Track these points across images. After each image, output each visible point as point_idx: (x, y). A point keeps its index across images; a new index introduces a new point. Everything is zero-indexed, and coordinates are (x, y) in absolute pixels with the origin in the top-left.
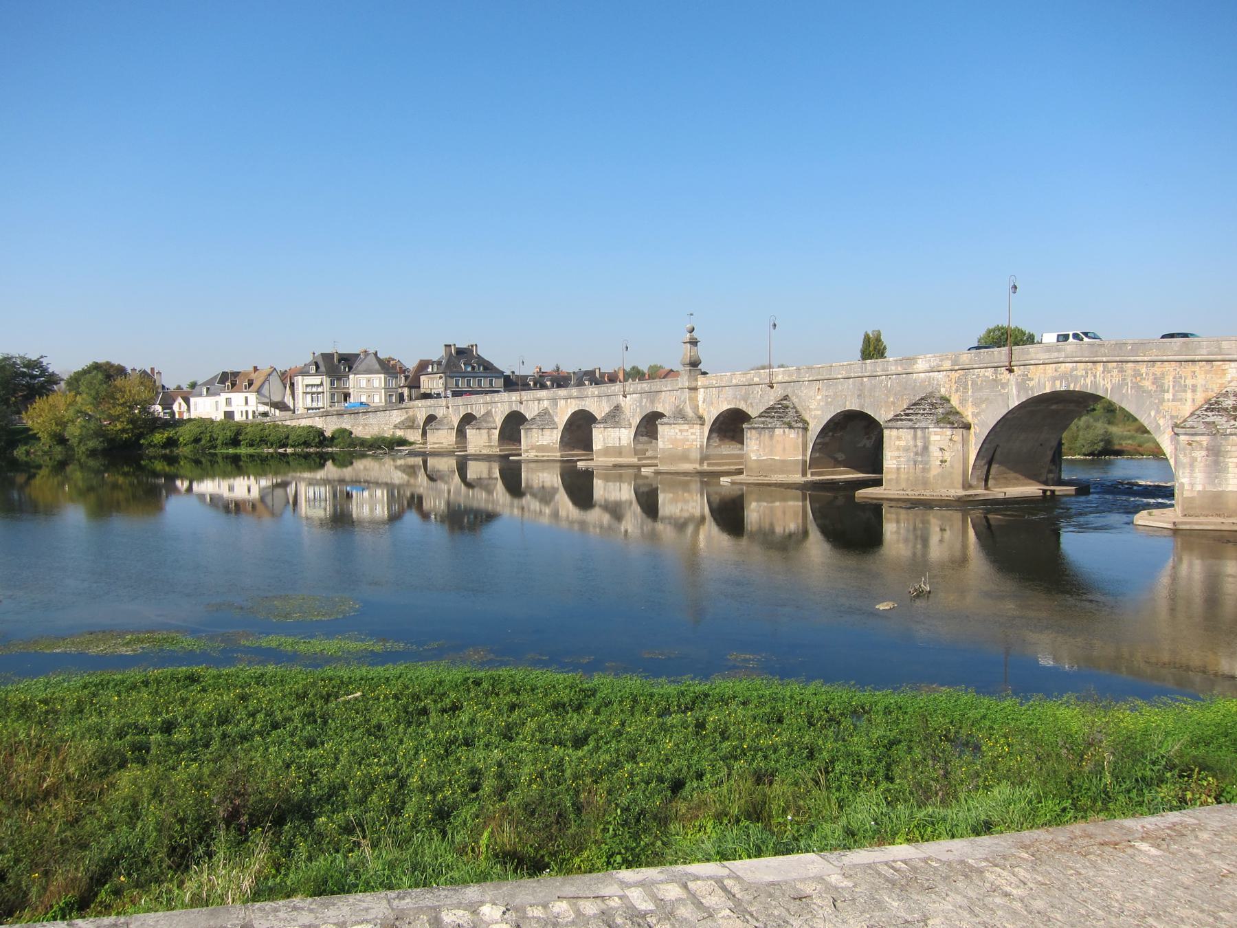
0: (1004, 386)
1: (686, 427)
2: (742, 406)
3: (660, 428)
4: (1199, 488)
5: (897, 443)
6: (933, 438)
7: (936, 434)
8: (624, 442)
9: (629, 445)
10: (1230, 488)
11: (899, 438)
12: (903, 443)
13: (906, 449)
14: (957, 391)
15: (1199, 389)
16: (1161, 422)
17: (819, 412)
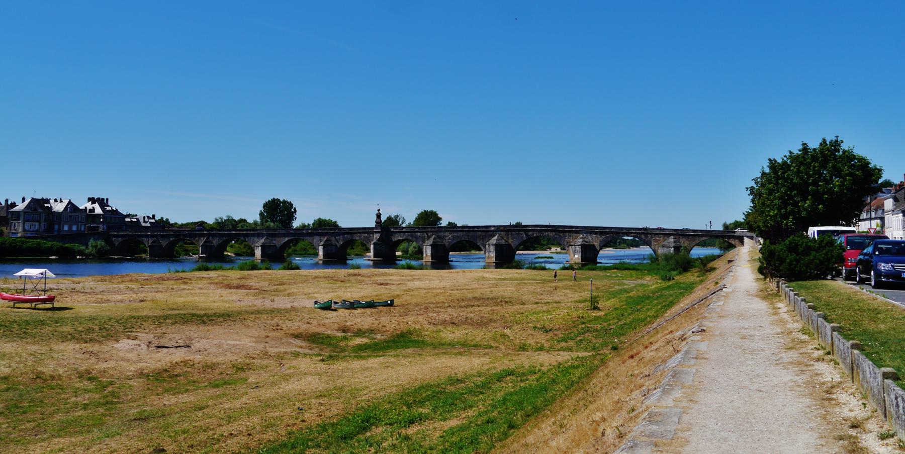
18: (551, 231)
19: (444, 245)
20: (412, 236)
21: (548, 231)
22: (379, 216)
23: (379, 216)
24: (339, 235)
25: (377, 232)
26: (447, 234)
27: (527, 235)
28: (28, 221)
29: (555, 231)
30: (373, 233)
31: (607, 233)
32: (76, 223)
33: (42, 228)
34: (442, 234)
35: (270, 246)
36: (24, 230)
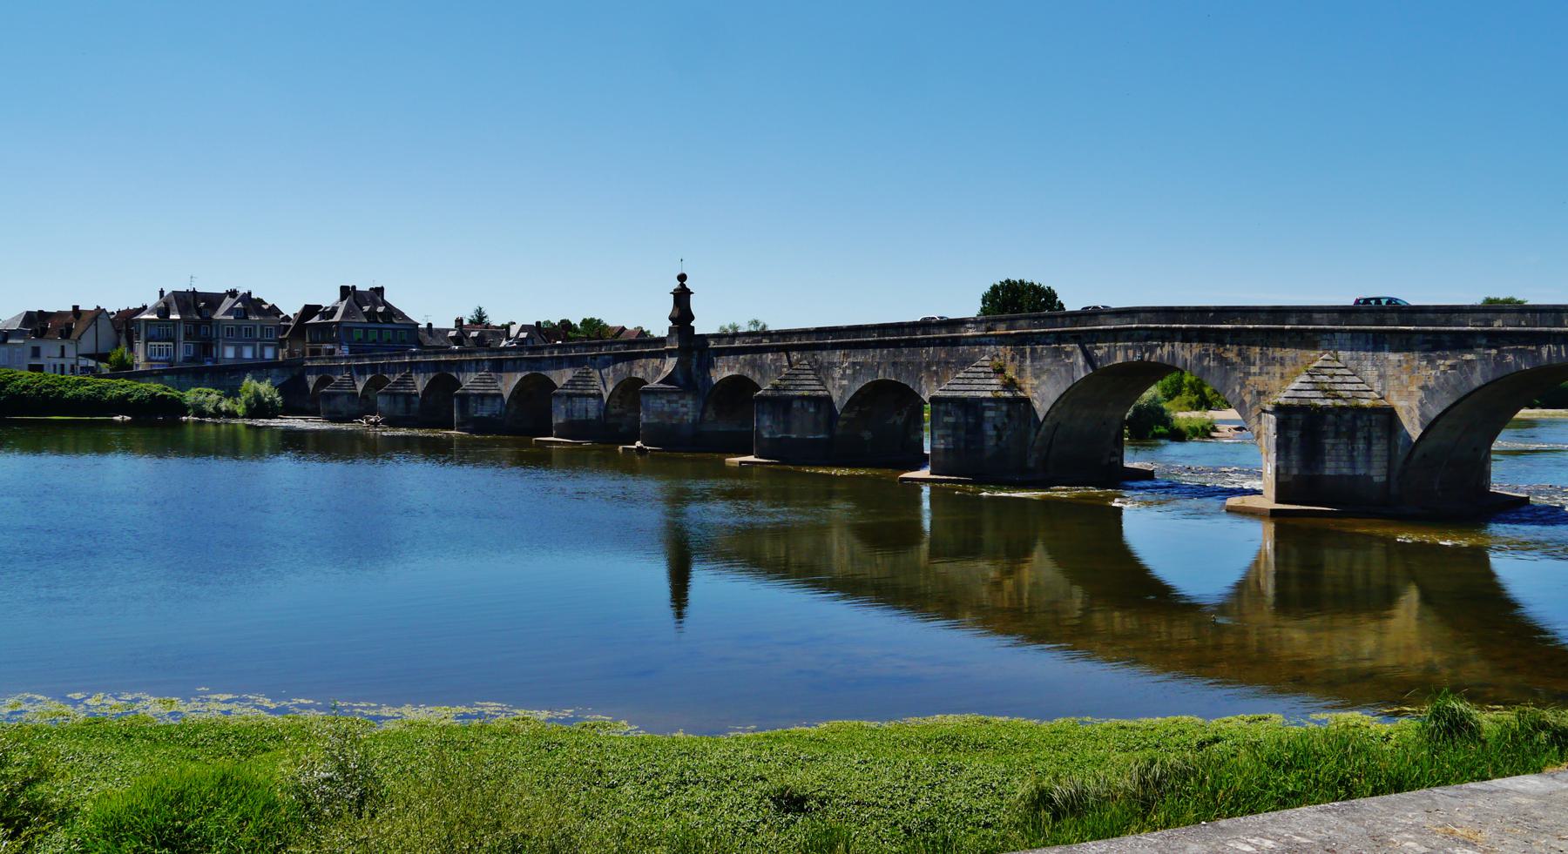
0: (1068, 355)
1: (675, 397)
2: (748, 373)
3: (643, 398)
4: (1295, 472)
5: (947, 419)
6: (989, 414)
7: (990, 409)
8: (592, 415)
9: (599, 417)
10: (1327, 472)
11: (947, 414)
12: (950, 420)
13: (955, 427)
14: (1013, 359)
15: (1288, 362)
16: (1248, 398)
17: (845, 382)
18: (1187, 337)
19: (829, 399)
20: (753, 365)
21: (1167, 336)
22: (162, 292)
23: (162, 292)
24: (606, 365)
25: (671, 353)
26: (837, 356)
27: (1089, 359)
28: (153, 339)
29: (1202, 336)
30: (661, 355)
31: (1462, 342)
32: (251, 341)
33: (181, 355)
34: (823, 356)
35: (482, 397)
36: (148, 360)
